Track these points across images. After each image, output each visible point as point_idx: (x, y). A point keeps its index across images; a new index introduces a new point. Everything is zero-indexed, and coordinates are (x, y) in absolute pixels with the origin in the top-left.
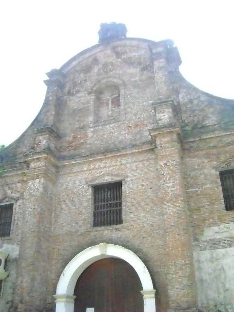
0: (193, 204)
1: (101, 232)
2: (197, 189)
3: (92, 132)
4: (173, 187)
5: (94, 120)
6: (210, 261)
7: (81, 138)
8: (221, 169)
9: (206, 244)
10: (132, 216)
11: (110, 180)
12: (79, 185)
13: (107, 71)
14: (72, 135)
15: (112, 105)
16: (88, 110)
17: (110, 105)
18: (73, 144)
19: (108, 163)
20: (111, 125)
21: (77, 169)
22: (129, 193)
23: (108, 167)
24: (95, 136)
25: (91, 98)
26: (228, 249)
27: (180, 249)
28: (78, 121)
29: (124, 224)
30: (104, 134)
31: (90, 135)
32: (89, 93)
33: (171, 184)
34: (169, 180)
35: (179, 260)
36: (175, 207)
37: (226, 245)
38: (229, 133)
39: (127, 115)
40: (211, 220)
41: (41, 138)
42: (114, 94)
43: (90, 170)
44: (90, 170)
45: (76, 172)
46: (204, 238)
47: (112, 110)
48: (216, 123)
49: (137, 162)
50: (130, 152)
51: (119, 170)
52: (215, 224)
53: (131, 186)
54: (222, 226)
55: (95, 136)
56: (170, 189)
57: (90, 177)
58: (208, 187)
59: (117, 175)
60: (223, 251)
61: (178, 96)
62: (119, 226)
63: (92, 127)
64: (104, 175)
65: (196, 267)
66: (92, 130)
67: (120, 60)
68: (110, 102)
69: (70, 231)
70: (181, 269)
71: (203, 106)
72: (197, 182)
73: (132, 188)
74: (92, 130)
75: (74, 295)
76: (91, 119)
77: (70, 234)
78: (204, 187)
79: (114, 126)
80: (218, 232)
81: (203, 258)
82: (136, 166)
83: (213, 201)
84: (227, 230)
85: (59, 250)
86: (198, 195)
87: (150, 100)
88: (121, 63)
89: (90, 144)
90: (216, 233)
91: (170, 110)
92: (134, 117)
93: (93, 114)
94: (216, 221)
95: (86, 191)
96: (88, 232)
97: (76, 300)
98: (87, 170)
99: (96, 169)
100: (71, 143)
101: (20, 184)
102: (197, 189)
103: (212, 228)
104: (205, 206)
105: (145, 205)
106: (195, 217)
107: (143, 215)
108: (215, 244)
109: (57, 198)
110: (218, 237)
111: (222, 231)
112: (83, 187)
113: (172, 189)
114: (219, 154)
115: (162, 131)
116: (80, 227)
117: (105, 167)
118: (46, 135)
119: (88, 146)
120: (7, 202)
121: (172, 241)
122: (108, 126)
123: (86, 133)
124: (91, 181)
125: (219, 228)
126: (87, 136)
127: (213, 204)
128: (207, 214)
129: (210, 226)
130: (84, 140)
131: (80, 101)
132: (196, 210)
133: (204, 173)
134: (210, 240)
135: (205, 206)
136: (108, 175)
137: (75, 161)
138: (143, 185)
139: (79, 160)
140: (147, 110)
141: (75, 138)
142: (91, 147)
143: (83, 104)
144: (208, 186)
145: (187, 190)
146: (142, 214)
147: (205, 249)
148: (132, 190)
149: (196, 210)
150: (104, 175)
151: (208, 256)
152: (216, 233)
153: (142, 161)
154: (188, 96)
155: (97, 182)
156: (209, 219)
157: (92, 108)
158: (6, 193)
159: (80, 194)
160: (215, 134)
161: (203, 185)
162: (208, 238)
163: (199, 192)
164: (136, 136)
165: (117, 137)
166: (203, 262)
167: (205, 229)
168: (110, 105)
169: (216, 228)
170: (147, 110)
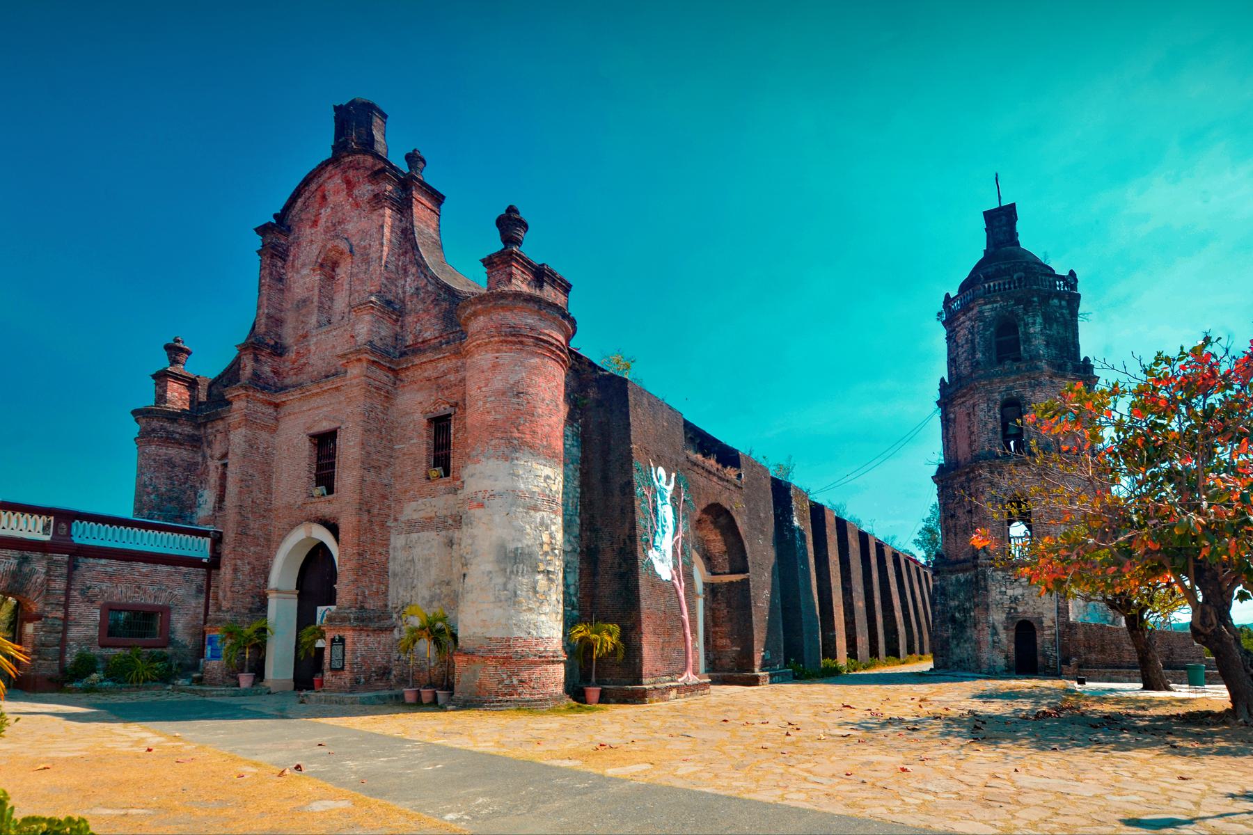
0: (398, 468)
8: (430, 415)
20: (334, 333)
29: (335, 495)
30: (326, 349)
31: (313, 348)
38: (441, 355)
43: (310, 410)
46: (403, 518)
48: (437, 335)
52: (414, 498)
65: (391, 556)
66: (315, 340)
70: (349, 560)
75: (297, 589)
77: (289, 507)
78: (412, 442)
81: (398, 545)
84: (423, 507)
86: (404, 454)
97: (298, 595)
108: (413, 526)
110: (416, 516)
124: (308, 428)
132: (400, 477)
144: (415, 441)
147: (401, 533)
149: (400, 477)
151: (404, 542)
154: (416, 283)
155: (317, 429)
169: (414, 504)
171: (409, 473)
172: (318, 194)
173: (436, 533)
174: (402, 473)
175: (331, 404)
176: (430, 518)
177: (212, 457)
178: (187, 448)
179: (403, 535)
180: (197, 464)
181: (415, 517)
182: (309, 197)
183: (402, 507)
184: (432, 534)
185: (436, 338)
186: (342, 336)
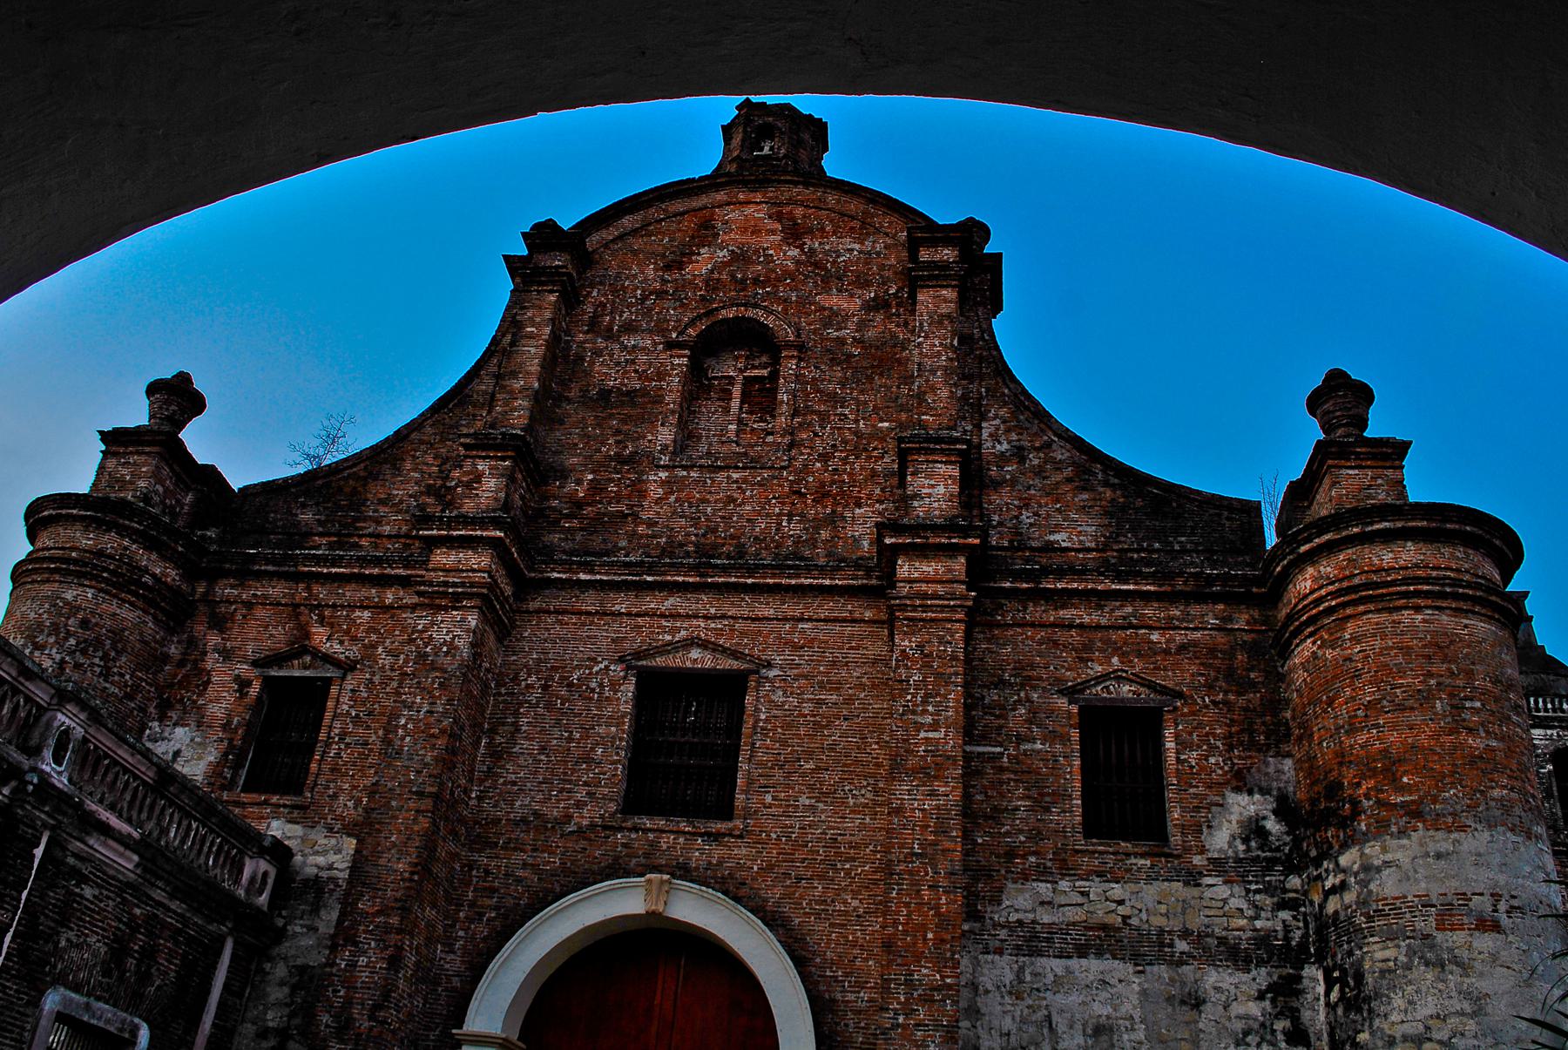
1: (651, 836)
2: (998, 749)
3: (663, 483)
4: (934, 727)
5: (675, 441)
6: (1010, 993)
7: (618, 498)
9: (1003, 934)
10: (768, 798)
11: (708, 664)
12: (594, 660)
13: (743, 280)
14: (590, 477)
15: (742, 403)
16: (658, 400)
17: (735, 404)
18: (588, 511)
19: (706, 604)
20: (735, 476)
21: (589, 602)
22: (767, 721)
23: (706, 617)
24: (672, 498)
25: (677, 361)
26: (1074, 963)
27: (930, 936)
28: (618, 432)
30: (704, 501)
31: (656, 491)
32: (670, 345)
33: (929, 719)
34: (925, 702)
35: (925, 971)
36: (933, 794)
37: (1070, 948)
39: (793, 452)
40: (1033, 859)
41: (482, 466)
42: (754, 367)
43: (638, 615)
44: (638, 615)
45: (588, 613)
47: (740, 422)
48: (1093, 545)
49: (810, 620)
50: (793, 582)
51: (743, 634)
52: (1043, 874)
53: (778, 697)
54: (1064, 885)
55: (672, 498)
56: (922, 735)
57: (637, 642)
58: (1039, 751)
59: (735, 654)
60: (1057, 965)
61: (980, 428)
62: (721, 826)
63: (665, 467)
64: (689, 643)
66: (663, 475)
67: (794, 252)
68: (737, 391)
69: (536, 814)
70: (927, 1000)
71: (1058, 477)
72: (1000, 727)
73: (780, 707)
74: (663, 475)
76: (666, 435)
78: (1028, 746)
79: (745, 481)
80: (1049, 903)
81: (986, 981)
82: (803, 631)
83: (1048, 799)
85: (487, 872)
86: (1002, 770)
87: (882, 420)
88: (798, 262)
89: (651, 524)
90: (1042, 903)
91: (955, 471)
92: (818, 465)
93: (673, 419)
94: (1049, 864)
95: (614, 686)
96: (605, 828)
98: (629, 614)
99: (663, 616)
100: (579, 504)
101: (367, 614)
102: (998, 749)
103: (1028, 885)
104: (1017, 809)
105: (818, 768)
106: (980, 841)
107: (807, 802)
108: (1032, 941)
109: (503, 691)
111: (1063, 900)
112: (607, 667)
113: (931, 735)
114: (1087, 647)
115: (927, 538)
116: (579, 805)
117: (696, 617)
118: (503, 459)
119: (641, 529)
120: (306, 668)
121: (907, 905)
122: (721, 476)
123: (640, 481)
124: (638, 655)
125: (1054, 891)
126: (643, 494)
127: (1047, 810)
128: (1023, 839)
129: (1025, 877)
130: (631, 507)
131: (633, 362)
132: (986, 817)
133: (1029, 700)
134: (1020, 922)
135: (1017, 809)
136: (704, 645)
137: (592, 572)
138: (820, 703)
139: (606, 574)
140: (865, 450)
141: (596, 488)
142: (654, 536)
143: (642, 376)
144: (1039, 746)
145: (968, 748)
146: (804, 800)
147: (1000, 952)
148: (778, 713)
150: (689, 643)
152: (1042, 903)
153: (826, 620)
155: (659, 661)
156: (1024, 857)
157: (672, 399)
158: (308, 635)
159: (593, 690)
160: (1086, 581)
161: (1020, 739)
162: (1014, 917)
163: (1005, 760)
164: (817, 529)
165: (749, 520)
166: (987, 992)
167: (1010, 885)
168: (735, 404)
169: (1044, 888)
170: (865, 450)
171: (1020, 814)
172: (689, 224)
173: (1130, 968)
174: (995, 809)
175: (724, 617)
176: (1104, 927)
177: (226, 655)
178: (160, 616)
179: (1006, 958)
180: (166, 658)
181: (1046, 919)
182: (662, 220)
183: (1001, 890)
184: (1120, 969)
185: (1088, 550)
186: (760, 484)
